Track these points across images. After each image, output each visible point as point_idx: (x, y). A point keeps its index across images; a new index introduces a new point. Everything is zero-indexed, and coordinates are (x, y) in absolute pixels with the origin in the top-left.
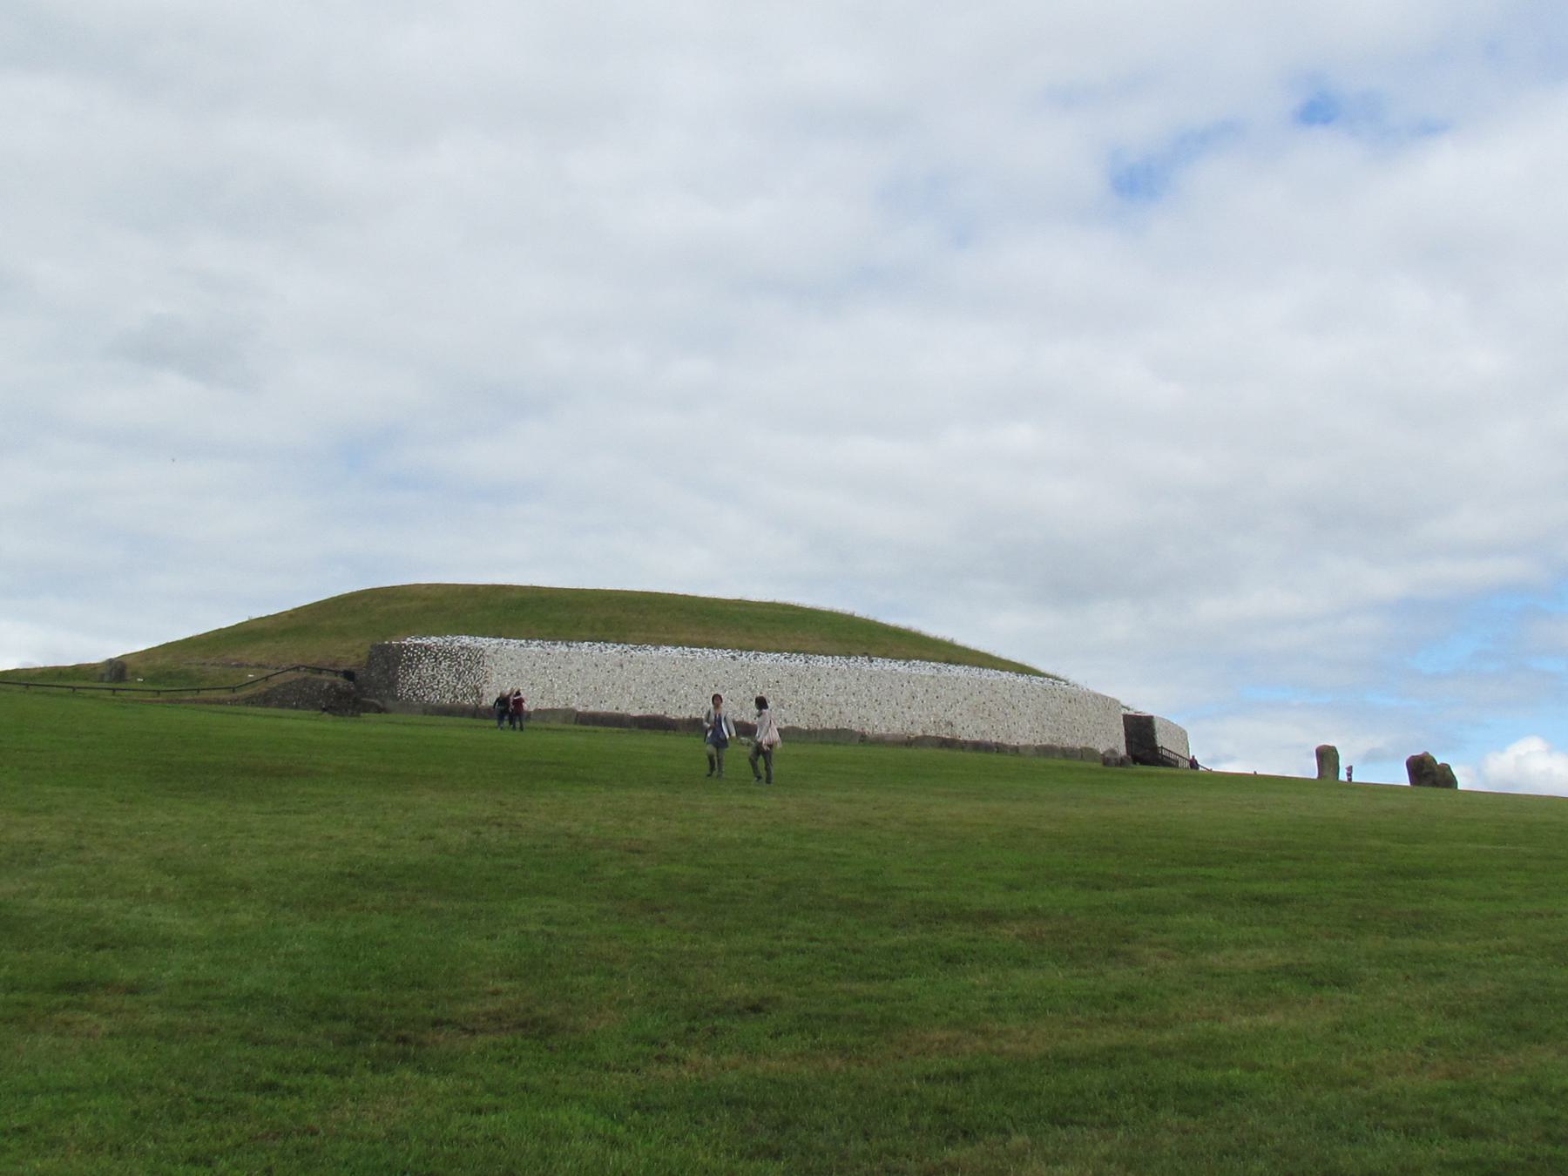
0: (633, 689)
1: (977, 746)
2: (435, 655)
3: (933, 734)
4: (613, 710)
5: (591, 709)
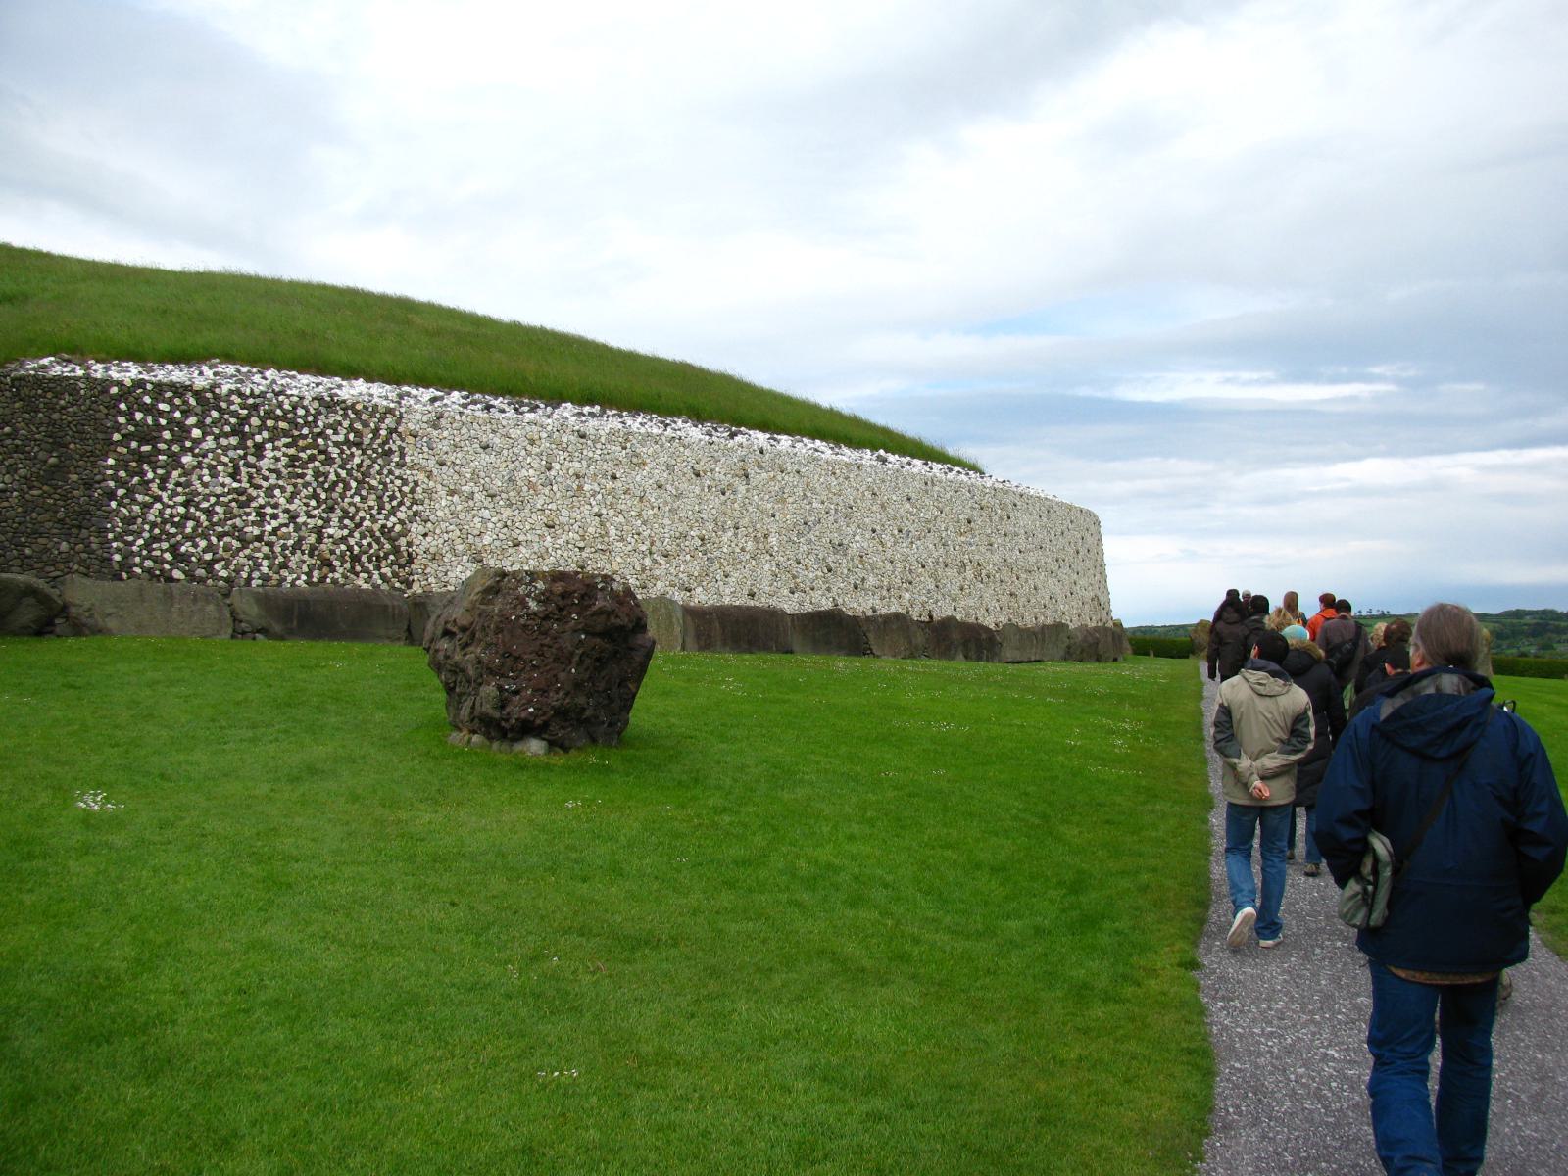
0: (773, 540)
2: (247, 424)
4: (742, 600)
5: (701, 597)
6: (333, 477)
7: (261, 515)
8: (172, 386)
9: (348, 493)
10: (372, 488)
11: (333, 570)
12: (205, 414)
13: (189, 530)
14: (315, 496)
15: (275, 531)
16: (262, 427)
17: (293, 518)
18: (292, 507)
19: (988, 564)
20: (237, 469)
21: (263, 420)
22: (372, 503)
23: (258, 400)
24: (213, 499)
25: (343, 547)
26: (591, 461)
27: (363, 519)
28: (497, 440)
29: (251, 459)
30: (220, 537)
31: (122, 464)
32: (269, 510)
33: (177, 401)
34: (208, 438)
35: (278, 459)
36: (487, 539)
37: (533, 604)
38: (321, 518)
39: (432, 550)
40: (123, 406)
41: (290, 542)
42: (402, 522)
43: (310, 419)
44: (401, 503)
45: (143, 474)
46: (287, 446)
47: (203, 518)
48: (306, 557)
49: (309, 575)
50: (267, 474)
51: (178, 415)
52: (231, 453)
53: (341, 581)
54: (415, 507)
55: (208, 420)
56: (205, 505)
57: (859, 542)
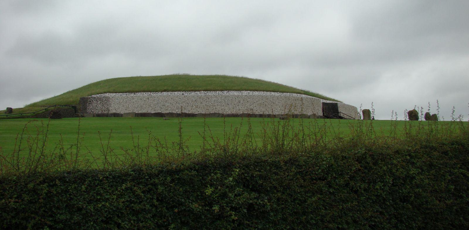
0: (152, 105)
1: (261, 116)
3: (246, 113)
4: (146, 112)
5: (140, 112)
19: (200, 105)
28: (118, 98)
31: (88, 104)
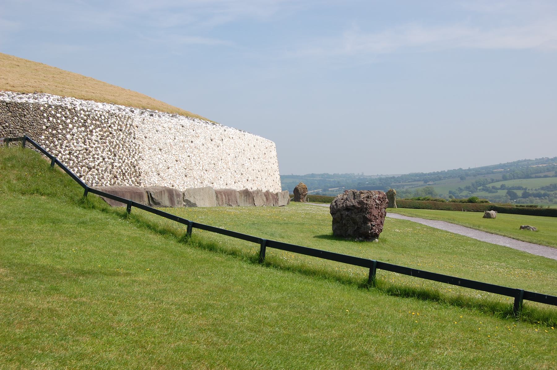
0: (230, 164)
2: (88, 122)
4: (224, 187)
6: (115, 143)
7: (94, 158)
8: (61, 106)
9: (120, 149)
10: (127, 147)
11: (118, 179)
12: (73, 118)
13: (71, 164)
14: (110, 151)
15: (98, 165)
16: (92, 124)
17: (104, 159)
18: (103, 155)
20: (85, 140)
21: (92, 120)
22: (127, 153)
23: (89, 113)
24: (78, 152)
25: (120, 170)
26: (186, 136)
27: (125, 159)
28: (160, 128)
29: (89, 136)
30: (82, 167)
31: (48, 139)
32: (96, 156)
33: (63, 113)
34: (75, 128)
35: (97, 136)
36: (161, 166)
37: (378, 202)
38: (113, 159)
39: (146, 171)
40: (45, 115)
41: (104, 169)
42: (136, 160)
43: (106, 120)
44: (136, 153)
45: (54, 142)
46: (100, 131)
47: (75, 160)
48: (109, 174)
49: (110, 181)
50: (94, 142)
51: (64, 118)
52: (83, 134)
53: (120, 183)
54: (140, 154)
55: (74, 121)
56: (75, 154)
57: (247, 164)
